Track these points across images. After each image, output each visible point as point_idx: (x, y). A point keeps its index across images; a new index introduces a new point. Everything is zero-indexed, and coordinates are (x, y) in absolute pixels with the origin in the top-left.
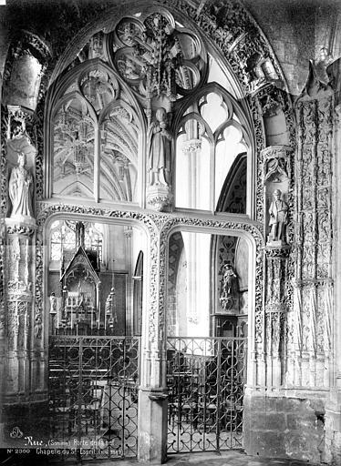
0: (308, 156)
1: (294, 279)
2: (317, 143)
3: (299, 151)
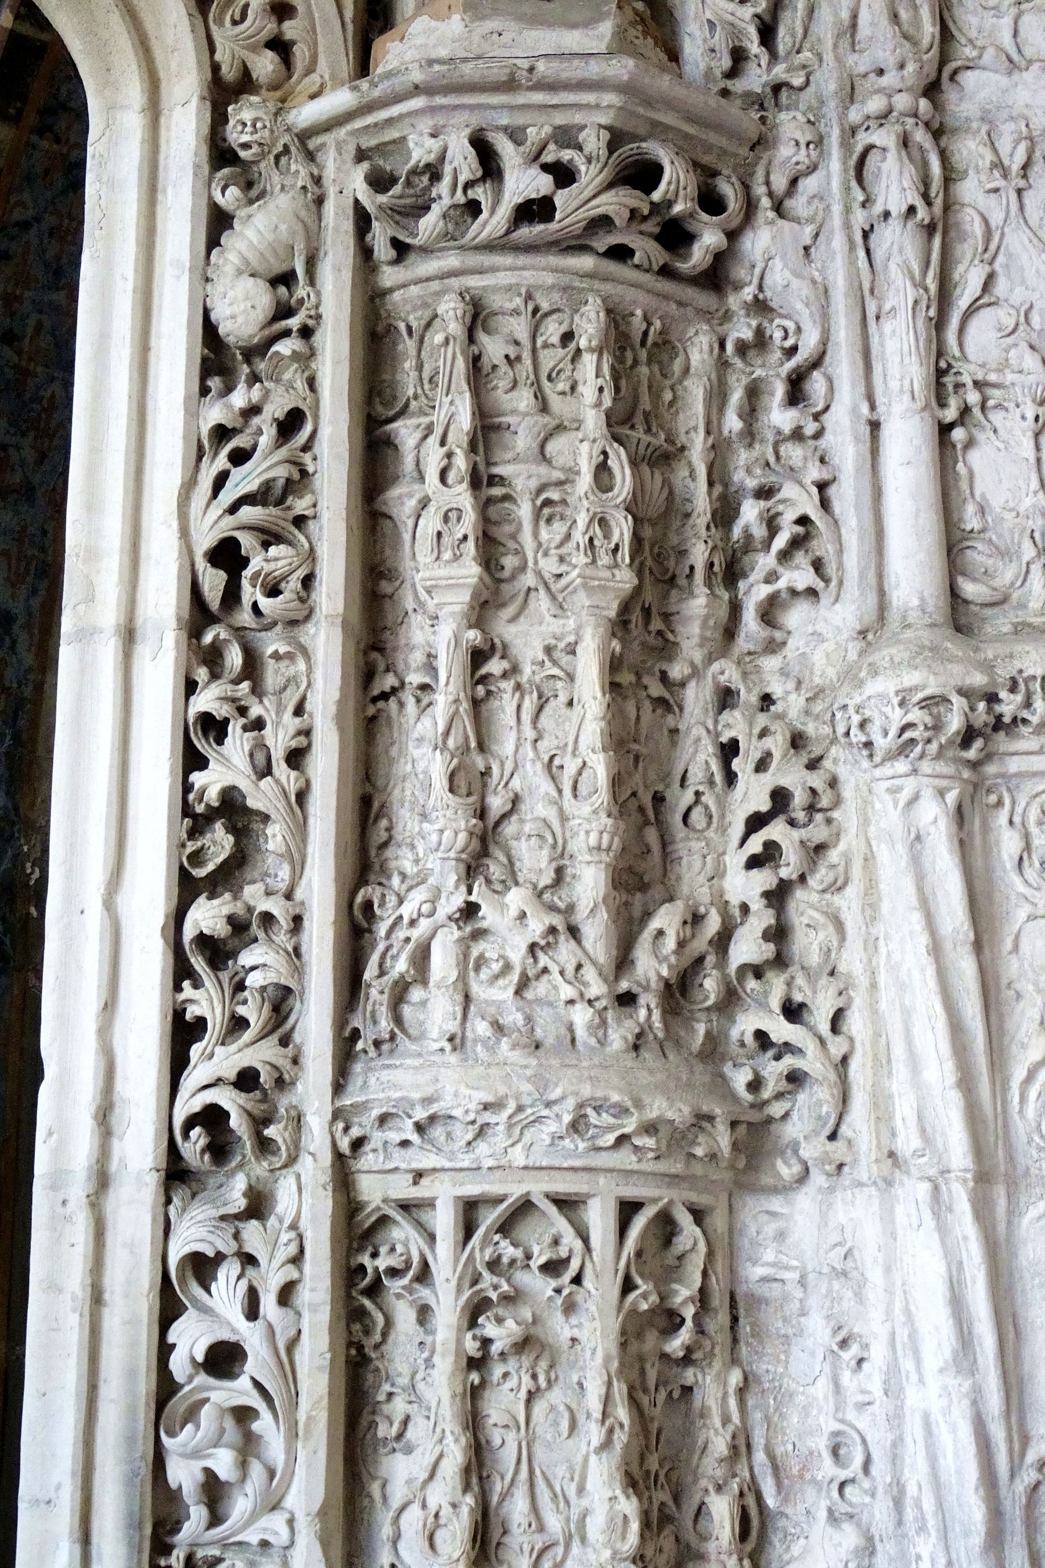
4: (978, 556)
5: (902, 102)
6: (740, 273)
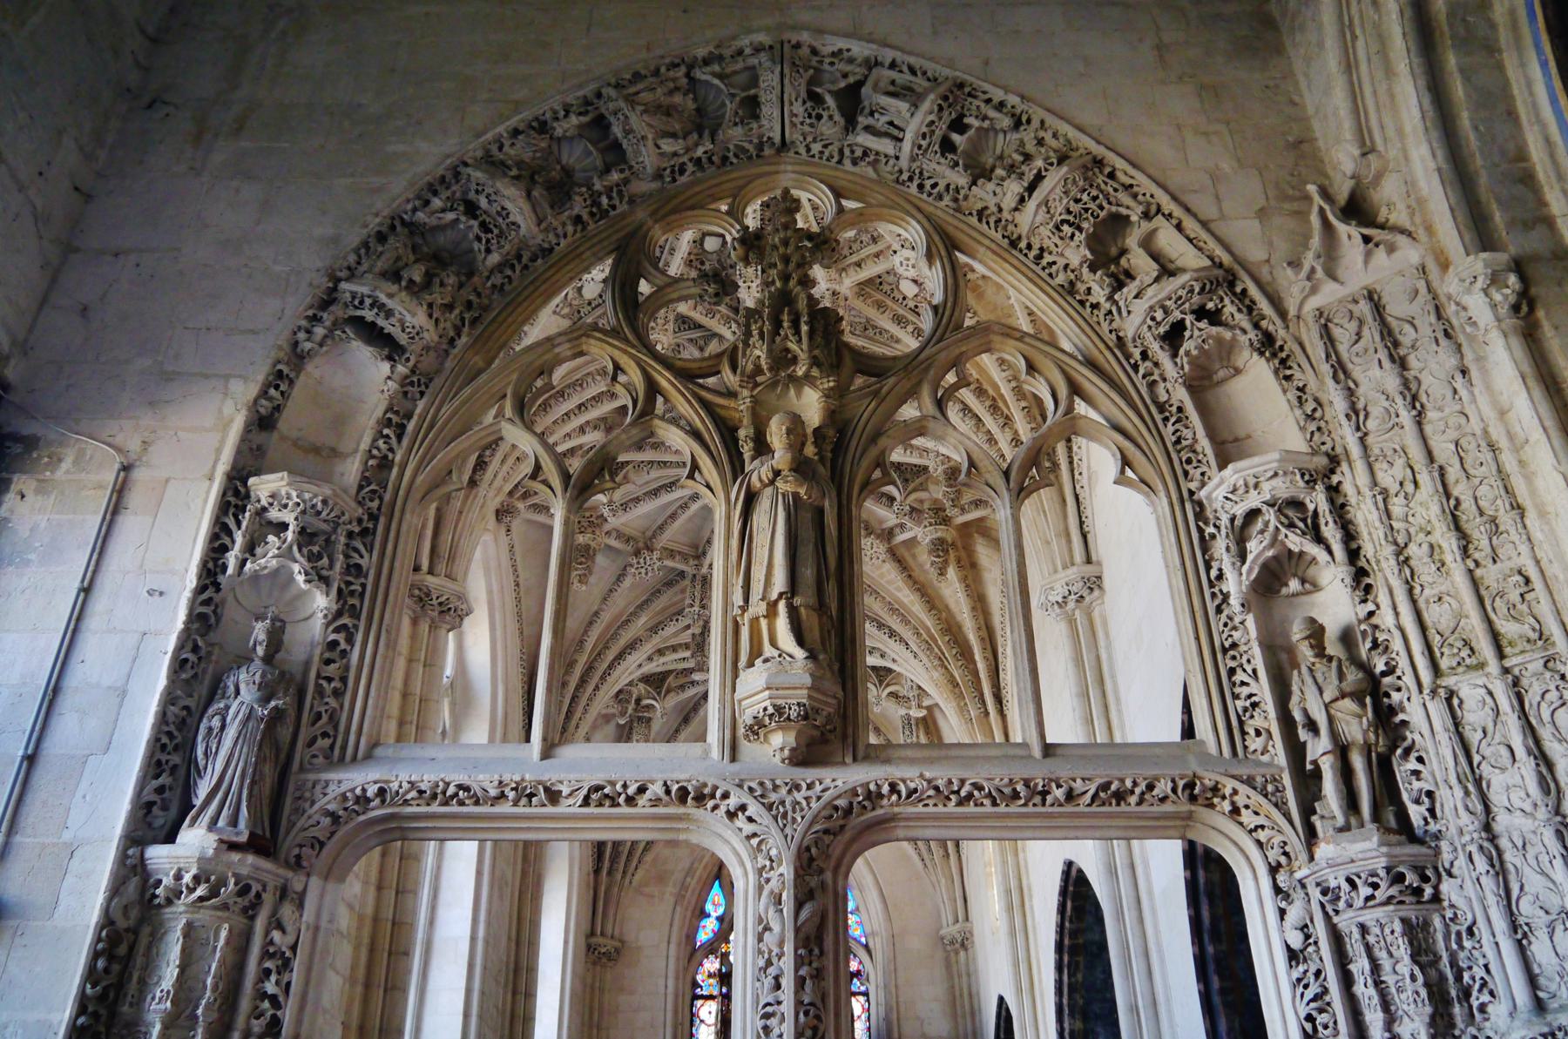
0: (1399, 470)
1: (1498, 1011)
2: (1419, 422)
3: (1360, 466)
4: (1542, 981)
5: (1476, 835)
6: (1442, 897)
